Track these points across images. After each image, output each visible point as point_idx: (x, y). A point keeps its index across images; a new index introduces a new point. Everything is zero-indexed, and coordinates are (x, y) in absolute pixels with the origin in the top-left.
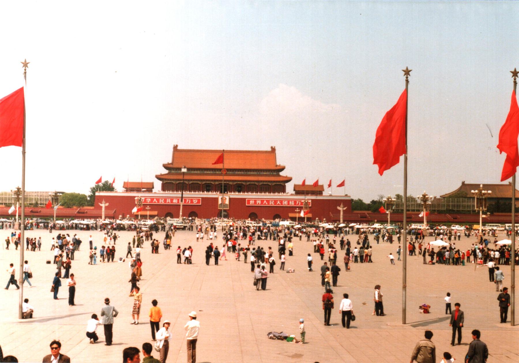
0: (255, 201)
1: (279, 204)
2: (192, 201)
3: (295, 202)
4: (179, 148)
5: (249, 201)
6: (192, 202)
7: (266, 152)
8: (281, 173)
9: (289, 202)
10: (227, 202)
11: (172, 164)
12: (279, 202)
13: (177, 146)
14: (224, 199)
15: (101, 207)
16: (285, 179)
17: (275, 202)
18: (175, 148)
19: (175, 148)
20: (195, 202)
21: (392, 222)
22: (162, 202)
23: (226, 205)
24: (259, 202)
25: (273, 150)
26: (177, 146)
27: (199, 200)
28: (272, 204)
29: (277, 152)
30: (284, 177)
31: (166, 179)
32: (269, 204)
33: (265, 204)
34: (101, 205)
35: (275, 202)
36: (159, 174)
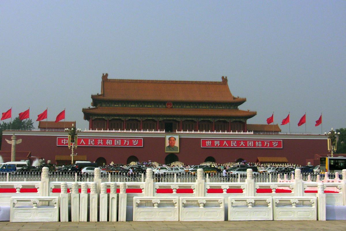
0: (213, 142)
1: (242, 146)
2: (131, 141)
3: (263, 143)
4: (109, 78)
5: (204, 142)
6: (131, 143)
7: (215, 83)
8: (240, 107)
9: (255, 142)
10: (177, 144)
11: (103, 95)
12: (242, 143)
13: (107, 75)
14: (174, 139)
15: (11, 145)
16: (245, 114)
17: (238, 142)
18: (105, 78)
19: (105, 78)
20: (135, 143)
21: (284, 170)
22: (91, 143)
23: (174, 148)
24: (217, 143)
25: (225, 80)
26: (107, 75)
27: (140, 141)
28: (234, 144)
29: (229, 83)
30: (244, 112)
31: (95, 115)
32: (230, 145)
33: (225, 145)
34: (8, 142)
35: (238, 142)
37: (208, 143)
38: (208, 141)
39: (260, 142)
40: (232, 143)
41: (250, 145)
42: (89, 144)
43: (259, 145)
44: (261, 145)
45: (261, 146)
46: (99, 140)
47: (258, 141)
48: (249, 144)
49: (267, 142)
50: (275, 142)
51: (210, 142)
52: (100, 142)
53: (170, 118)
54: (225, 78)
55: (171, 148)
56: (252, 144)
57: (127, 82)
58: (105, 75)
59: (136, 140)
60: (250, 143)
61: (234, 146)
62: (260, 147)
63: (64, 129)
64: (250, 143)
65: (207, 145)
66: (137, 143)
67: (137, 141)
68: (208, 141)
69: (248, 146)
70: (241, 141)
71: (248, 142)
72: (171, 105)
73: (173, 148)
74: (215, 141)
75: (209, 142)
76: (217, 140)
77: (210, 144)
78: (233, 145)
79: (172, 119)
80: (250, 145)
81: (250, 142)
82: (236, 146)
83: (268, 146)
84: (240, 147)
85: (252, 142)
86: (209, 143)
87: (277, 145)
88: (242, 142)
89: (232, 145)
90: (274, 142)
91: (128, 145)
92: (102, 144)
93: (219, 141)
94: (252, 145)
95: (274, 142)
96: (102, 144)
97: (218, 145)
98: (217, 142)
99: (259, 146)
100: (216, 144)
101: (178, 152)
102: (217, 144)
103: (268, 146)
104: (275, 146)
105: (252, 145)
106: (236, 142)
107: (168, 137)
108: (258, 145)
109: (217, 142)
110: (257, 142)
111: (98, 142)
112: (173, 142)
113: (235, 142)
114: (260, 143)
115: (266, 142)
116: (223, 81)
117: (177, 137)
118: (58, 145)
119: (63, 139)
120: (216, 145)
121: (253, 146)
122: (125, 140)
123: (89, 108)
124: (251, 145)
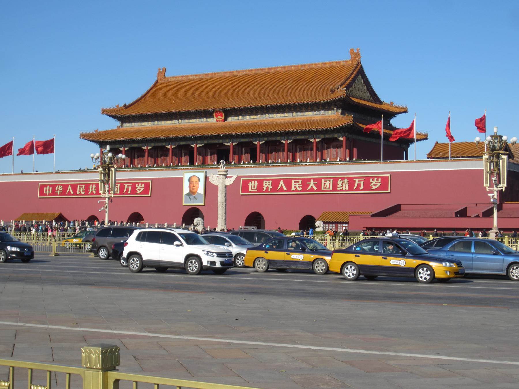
0: (260, 183)
1: (312, 189)
3: (351, 182)
9: (335, 180)
12: (312, 184)
17: (305, 182)
26: (165, 71)
35: (305, 182)
36: (90, 130)
37: (253, 186)
38: (253, 182)
39: (346, 179)
40: (293, 183)
41: (325, 188)
42: (78, 193)
43: (344, 185)
44: (347, 185)
45: (347, 189)
46: (91, 187)
47: (343, 179)
48: (324, 184)
49: (359, 181)
50: (375, 179)
51: (256, 184)
52: (92, 189)
53: (213, 140)
54: (356, 51)
55: (192, 197)
56: (330, 184)
57: (193, 80)
58: (161, 70)
59: (142, 183)
60: (327, 184)
61: (296, 190)
62: (345, 190)
63: (482, 156)
64: (327, 184)
65: (250, 190)
66: (142, 189)
67: (143, 185)
68: (253, 182)
69: (323, 189)
70: (309, 180)
71: (323, 180)
72: (222, 116)
73: (194, 197)
74: (264, 181)
75: (253, 184)
76: (267, 178)
77: (256, 188)
78: (295, 187)
79: (216, 141)
80: (325, 188)
81: (326, 181)
82: (301, 189)
83: (361, 188)
84: (309, 191)
85: (331, 180)
86: (254, 187)
87: (379, 184)
88: (312, 180)
89: (293, 189)
90: (373, 180)
91: (129, 192)
92: (95, 192)
93: (271, 181)
94: (329, 187)
95: (373, 180)
96: (95, 192)
97: (269, 190)
98: (267, 183)
99: (344, 189)
100: (266, 186)
101: (203, 204)
102: (267, 188)
103: (361, 188)
104: (374, 187)
105: (329, 187)
106: (300, 181)
107: (186, 175)
108: (342, 186)
109: (267, 183)
110: (340, 180)
111: (89, 189)
112: (195, 185)
113: (298, 182)
114: (346, 182)
115: (357, 180)
116: (352, 60)
117: (201, 175)
118: (40, 195)
119: (46, 186)
120: (265, 190)
121: (331, 189)
122: (126, 185)
123: (96, 131)
124: (328, 187)
